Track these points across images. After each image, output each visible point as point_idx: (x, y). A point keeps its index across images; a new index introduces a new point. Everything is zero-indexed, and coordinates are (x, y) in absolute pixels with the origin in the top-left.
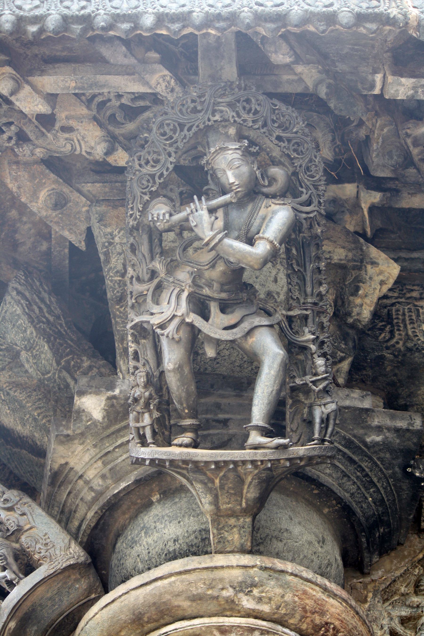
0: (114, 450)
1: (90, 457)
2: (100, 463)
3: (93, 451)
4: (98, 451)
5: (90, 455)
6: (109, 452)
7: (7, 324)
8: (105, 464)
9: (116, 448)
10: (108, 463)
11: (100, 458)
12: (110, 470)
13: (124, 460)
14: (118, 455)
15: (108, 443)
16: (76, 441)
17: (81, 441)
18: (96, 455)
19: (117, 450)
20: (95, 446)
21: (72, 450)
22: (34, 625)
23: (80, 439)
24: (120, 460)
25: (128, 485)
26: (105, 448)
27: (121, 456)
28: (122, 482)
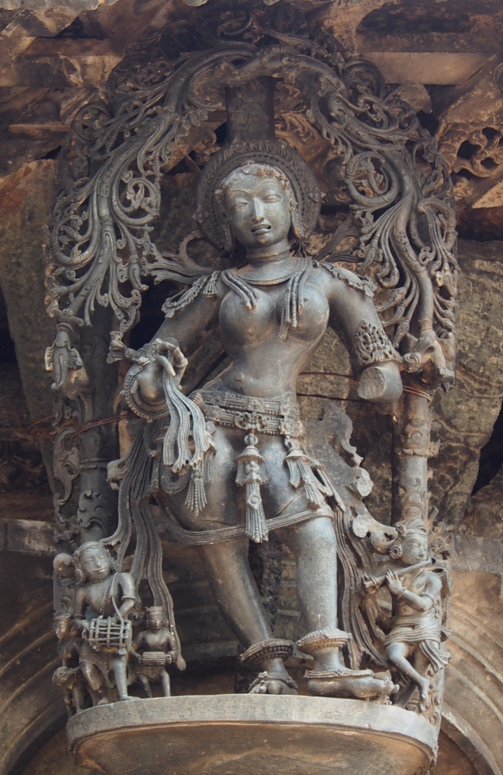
0: (488, 673)
1: (461, 633)
2: (459, 656)
3: (472, 635)
4: (476, 643)
5: (466, 632)
6: (484, 666)
7: (476, 297)
8: (460, 666)
9: (493, 676)
10: (465, 671)
11: (469, 655)
12: (460, 682)
13: (480, 699)
14: (482, 683)
15: (494, 657)
16: (484, 604)
17: (485, 611)
18: (468, 643)
19: (488, 678)
20: (483, 638)
21: (465, 597)
22: (349, 761)
23: (492, 610)
24: (476, 689)
25: (457, 730)
26: (482, 655)
27: (481, 689)
28: (454, 714)
